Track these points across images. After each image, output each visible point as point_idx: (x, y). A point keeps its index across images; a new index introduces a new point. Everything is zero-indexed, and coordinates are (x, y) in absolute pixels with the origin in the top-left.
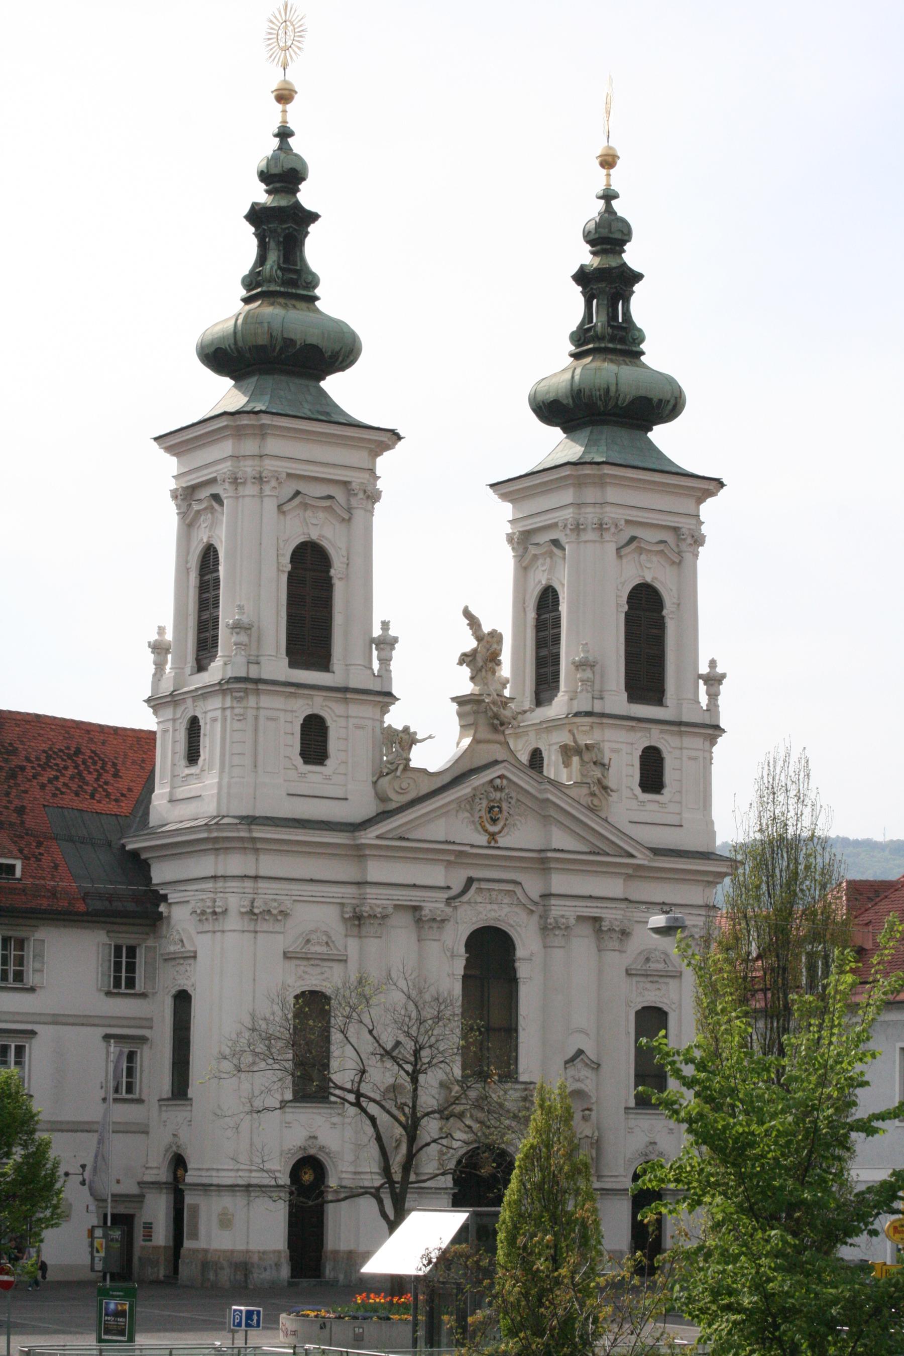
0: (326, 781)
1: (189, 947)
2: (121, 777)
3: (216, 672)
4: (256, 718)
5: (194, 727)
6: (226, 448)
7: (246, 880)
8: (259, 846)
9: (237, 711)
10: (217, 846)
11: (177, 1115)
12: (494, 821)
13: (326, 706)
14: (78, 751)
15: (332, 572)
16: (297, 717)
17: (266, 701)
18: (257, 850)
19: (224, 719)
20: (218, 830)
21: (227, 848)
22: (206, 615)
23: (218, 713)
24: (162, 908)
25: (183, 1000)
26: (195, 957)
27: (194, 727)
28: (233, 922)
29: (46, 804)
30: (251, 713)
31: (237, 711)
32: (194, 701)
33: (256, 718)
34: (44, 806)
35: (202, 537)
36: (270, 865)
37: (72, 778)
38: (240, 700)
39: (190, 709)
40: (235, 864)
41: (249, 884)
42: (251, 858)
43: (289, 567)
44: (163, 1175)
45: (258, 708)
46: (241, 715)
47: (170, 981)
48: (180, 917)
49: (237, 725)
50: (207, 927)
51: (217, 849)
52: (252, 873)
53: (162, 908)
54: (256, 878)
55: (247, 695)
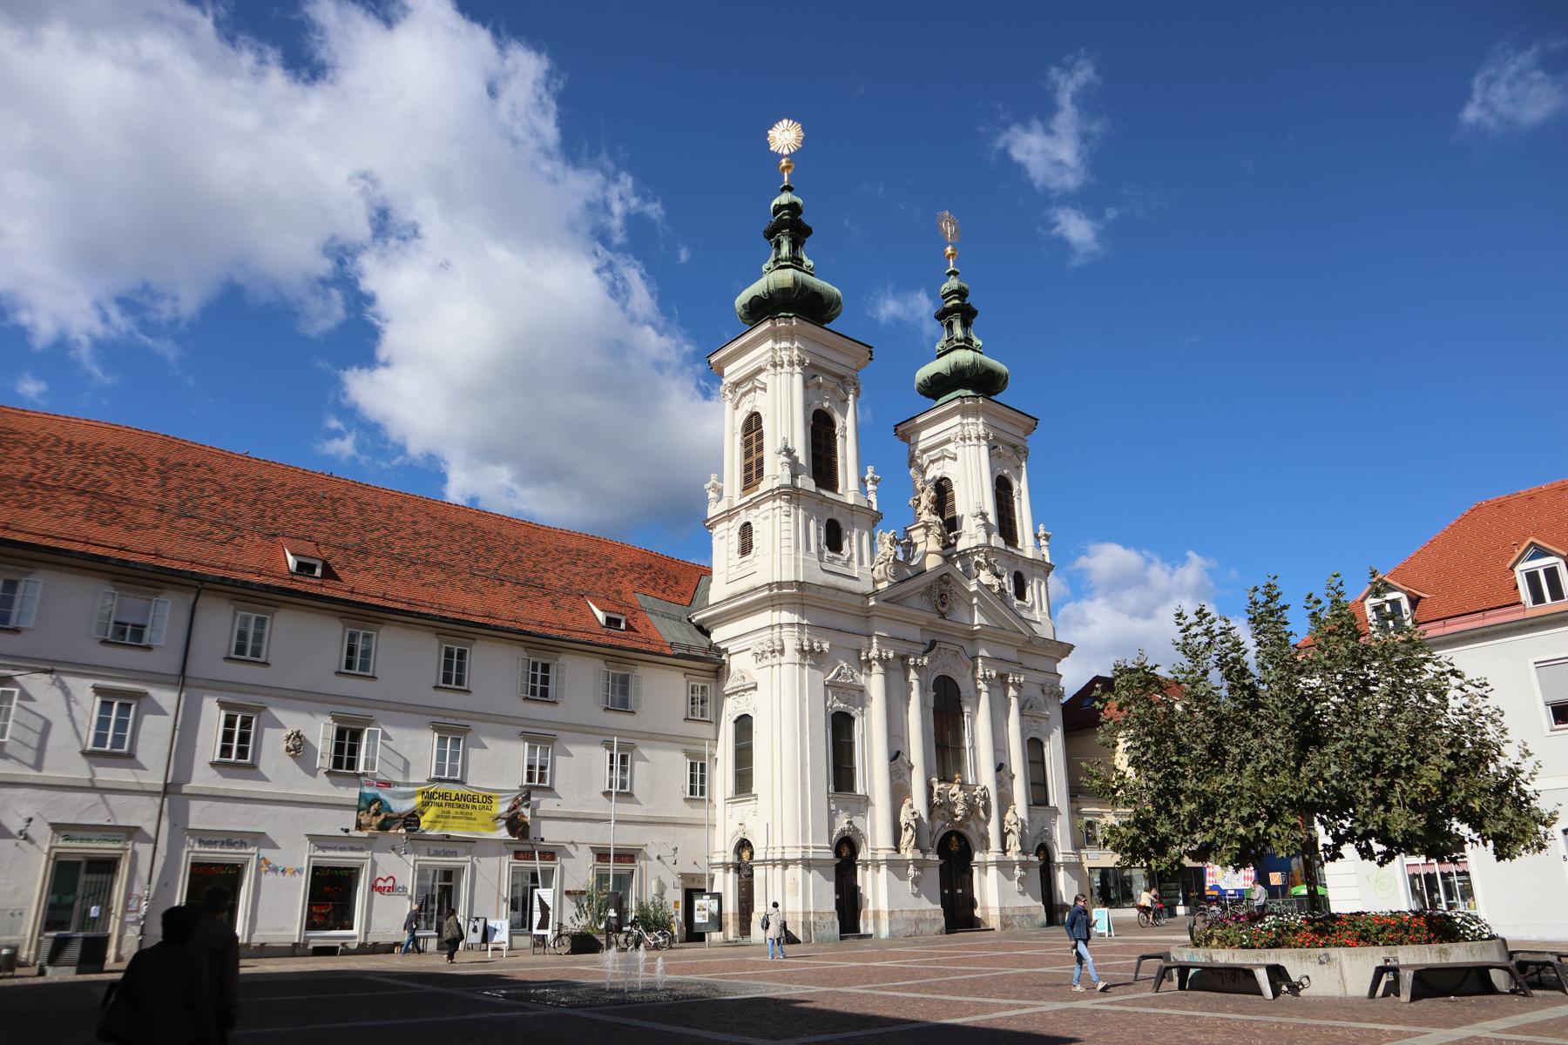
1: (748, 682)
3: (764, 486)
5: (746, 529)
11: (744, 809)
12: (943, 604)
14: (650, 567)
22: (755, 456)
24: (724, 657)
25: (744, 725)
26: (755, 688)
27: (746, 529)
28: (791, 654)
39: (744, 517)
44: (731, 858)
47: (732, 708)
48: (740, 665)
49: (785, 519)
50: (765, 662)
53: (724, 657)
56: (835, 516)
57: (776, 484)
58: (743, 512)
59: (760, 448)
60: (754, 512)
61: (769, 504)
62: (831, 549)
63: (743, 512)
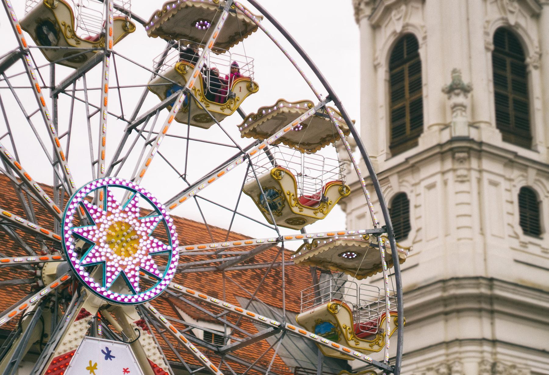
0: (544, 255)
2: (294, 285)
3: (428, 139)
4: (479, 181)
6: (254, 147)
7: (485, 343)
8: (497, 307)
9: (460, 172)
10: (449, 309)
13: (539, 180)
15: (528, 60)
16: (514, 186)
17: (486, 164)
18: (492, 312)
19: (445, 183)
20: (458, 286)
21: (458, 311)
23: (438, 179)
29: (236, 293)
30: (474, 175)
31: (460, 172)
32: (400, 177)
33: (479, 181)
34: (235, 295)
35: (395, 26)
36: (506, 330)
37: (253, 278)
38: (461, 160)
40: (471, 327)
41: (487, 348)
42: (486, 321)
43: (492, 47)
45: (480, 171)
46: (465, 176)
51: (446, 314)
52: (488, 335)
54: (494, 342)
55: (469, 157)
56: (531, 183)
57: (445, 136)
58: (394, 180)
59: (417, 85)
60: (410, 179)
61: (435, 167)
62: (526, 232)
63: (394, 180)
